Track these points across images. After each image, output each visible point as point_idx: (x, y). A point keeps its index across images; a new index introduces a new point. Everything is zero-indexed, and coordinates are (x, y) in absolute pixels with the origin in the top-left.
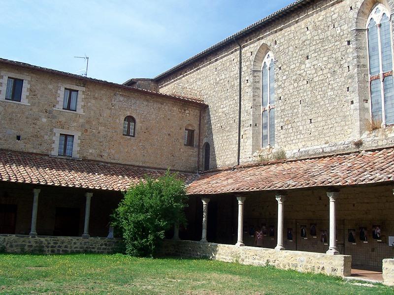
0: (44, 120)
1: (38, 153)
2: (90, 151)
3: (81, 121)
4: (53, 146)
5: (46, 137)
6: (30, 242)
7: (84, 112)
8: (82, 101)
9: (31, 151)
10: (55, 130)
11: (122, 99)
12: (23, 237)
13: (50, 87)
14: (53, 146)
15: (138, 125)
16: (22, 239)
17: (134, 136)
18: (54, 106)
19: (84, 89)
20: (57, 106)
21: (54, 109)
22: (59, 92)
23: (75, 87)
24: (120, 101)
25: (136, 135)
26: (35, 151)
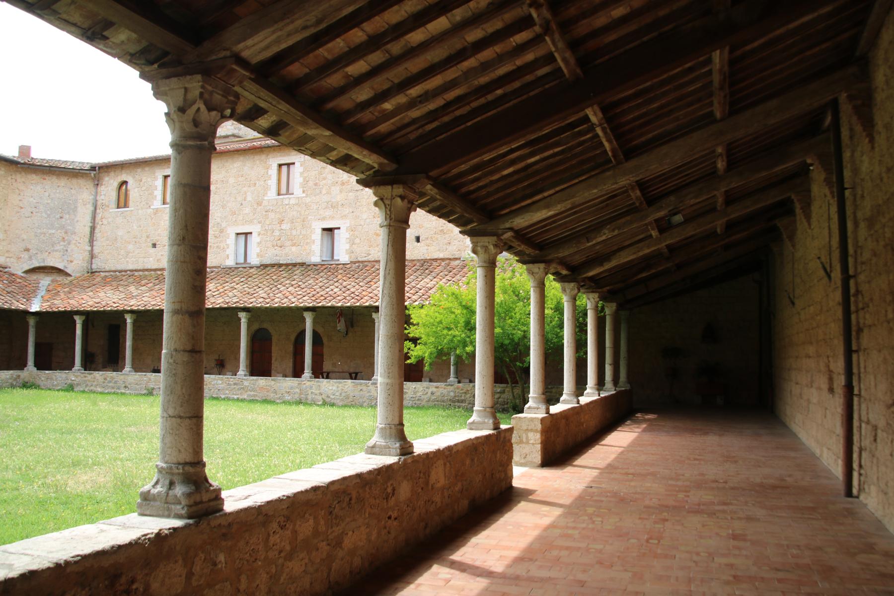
1: (446, 257)
6: (369, 392)
9: (436, 255)
12: (361, 384)
16: (359, 387)
26: (441, 256)
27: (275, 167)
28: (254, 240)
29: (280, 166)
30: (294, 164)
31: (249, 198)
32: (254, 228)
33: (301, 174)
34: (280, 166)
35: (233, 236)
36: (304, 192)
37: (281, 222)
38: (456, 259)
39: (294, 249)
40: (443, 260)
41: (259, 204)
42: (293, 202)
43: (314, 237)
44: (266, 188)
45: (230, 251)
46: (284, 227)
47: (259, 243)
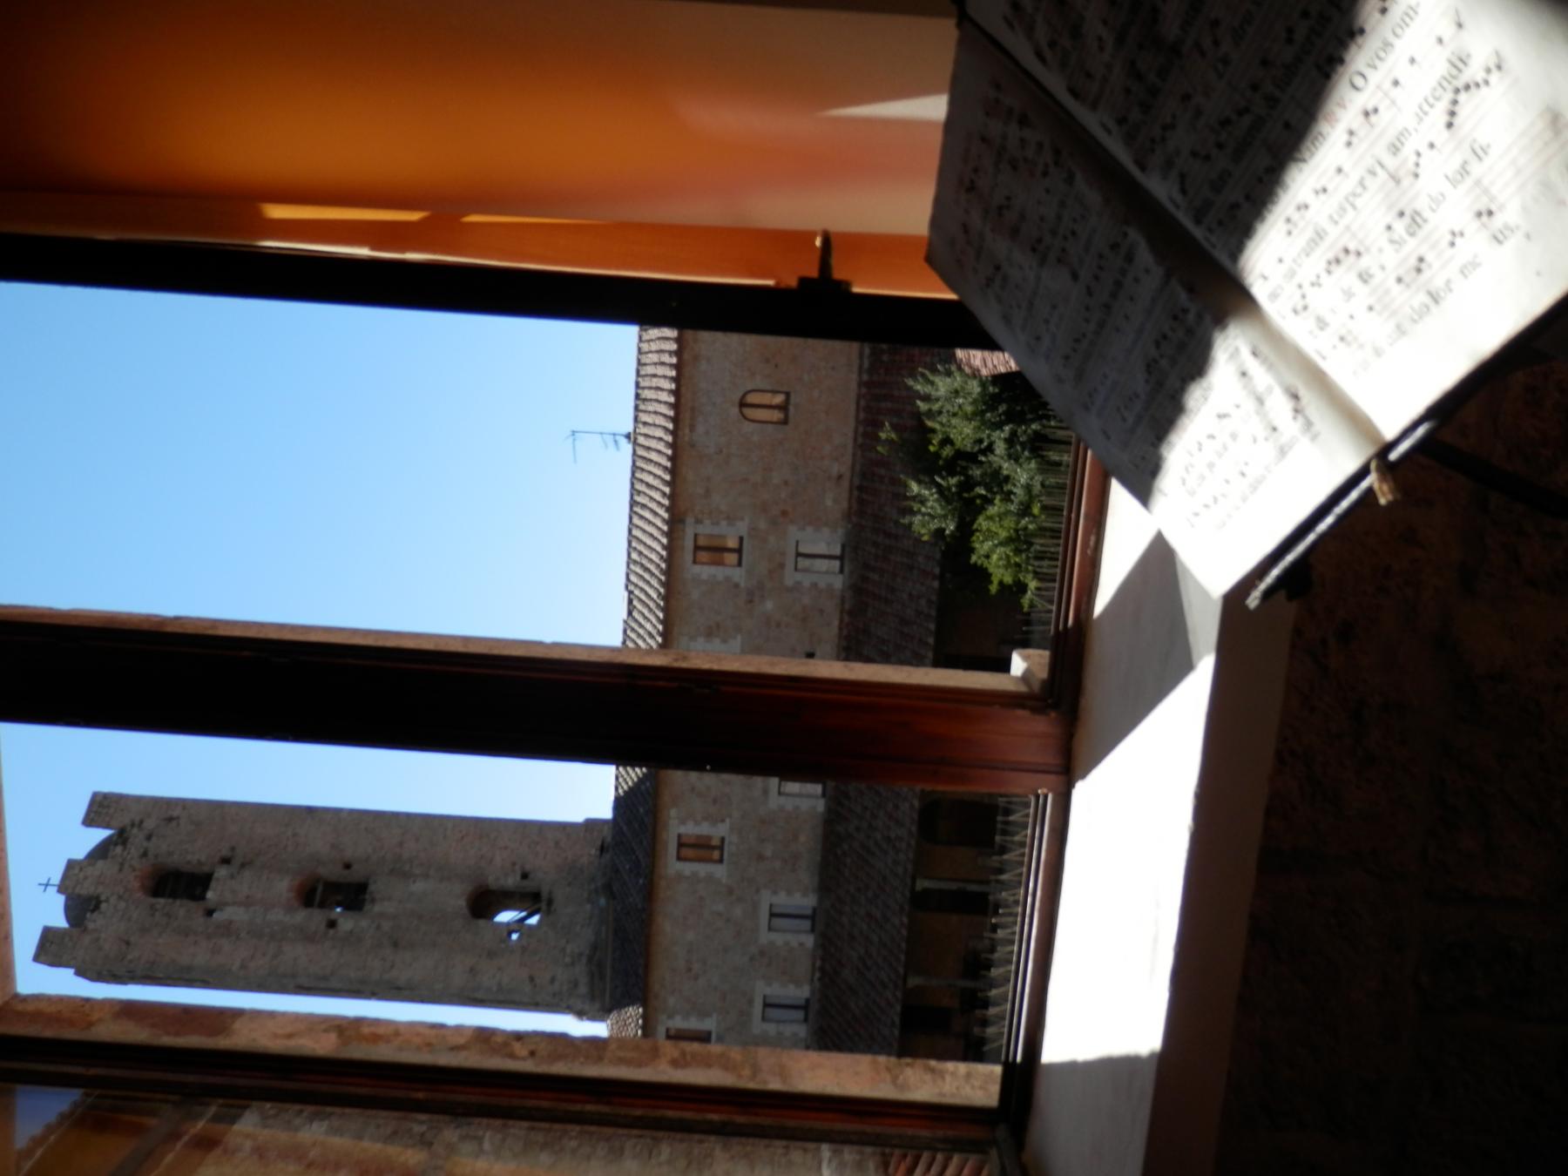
0: (769, 605)
2: (829, 503)
3: (763, 525)
4: (822, 585)
5: (806, 600)
7: (742, 519)
8: (717, 524)
10: (789, 582)
11: (700, 429)
13: (695, 595)
14: (822, 585)
15: (759, 383)
17: (788, 394)
18: (737, 586)
19: (690, 520)
20: (736, 579)
21: (742, 585)
22: (704, 577)
23: (689, 544)
24: (707, 433)
25: (785, 389)
26: (836, 623)
27: (680, 866)
28: (783, 900)
29: (679, 858)
30: (679, 836)
31: (720, 907)
32: (766, 899)
33: (697, 823)
34: (679, 858)
35: (774, 936)
36: (723, 821)
37: (761, 857)
38: (843, 602)
39: (802, 838)
40: (841, 621)
41: (730, 891)
42: (735, 839)
43: (789, 807)
44: (710, 879)
45: (793, 940)
46: (768, 853)
47: (789, 893)
